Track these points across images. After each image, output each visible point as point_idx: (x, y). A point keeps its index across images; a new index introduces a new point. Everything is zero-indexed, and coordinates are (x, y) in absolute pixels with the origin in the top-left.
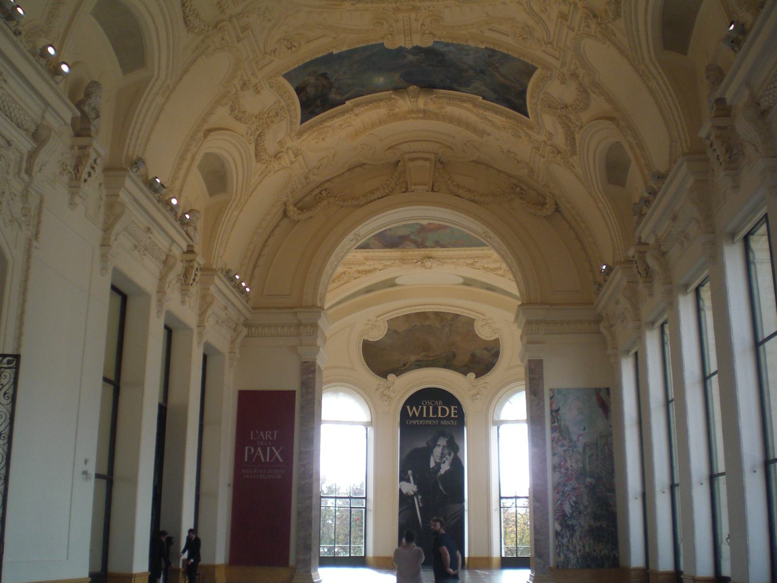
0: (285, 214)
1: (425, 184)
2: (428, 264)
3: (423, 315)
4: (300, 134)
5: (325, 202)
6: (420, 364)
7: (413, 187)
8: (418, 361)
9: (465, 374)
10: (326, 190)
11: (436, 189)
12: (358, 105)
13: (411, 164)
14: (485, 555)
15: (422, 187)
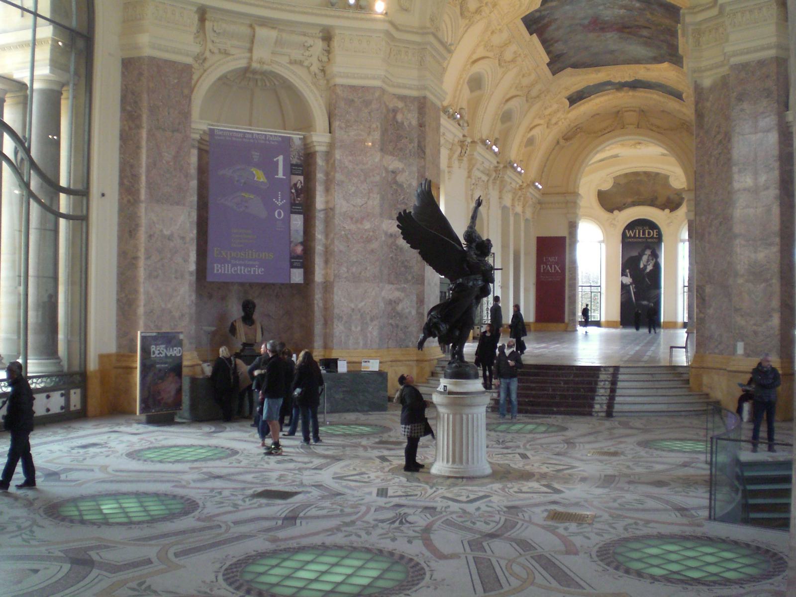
0: (558, 143)
1: (633, 125)
2: (638, 147)
3: (636, 174)
4: (568, 112)
5: (579, 135)
6: (634, 204)
7: (627, 126)
8: (633, 202)
9: (663, 209)
10: (579, 128)
11: (640, 127)
12: (597, 97)
13: (626, 114)
14: (673, 320)
15: (632, 126)
